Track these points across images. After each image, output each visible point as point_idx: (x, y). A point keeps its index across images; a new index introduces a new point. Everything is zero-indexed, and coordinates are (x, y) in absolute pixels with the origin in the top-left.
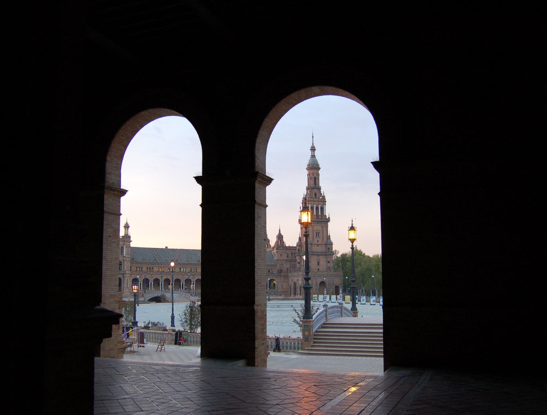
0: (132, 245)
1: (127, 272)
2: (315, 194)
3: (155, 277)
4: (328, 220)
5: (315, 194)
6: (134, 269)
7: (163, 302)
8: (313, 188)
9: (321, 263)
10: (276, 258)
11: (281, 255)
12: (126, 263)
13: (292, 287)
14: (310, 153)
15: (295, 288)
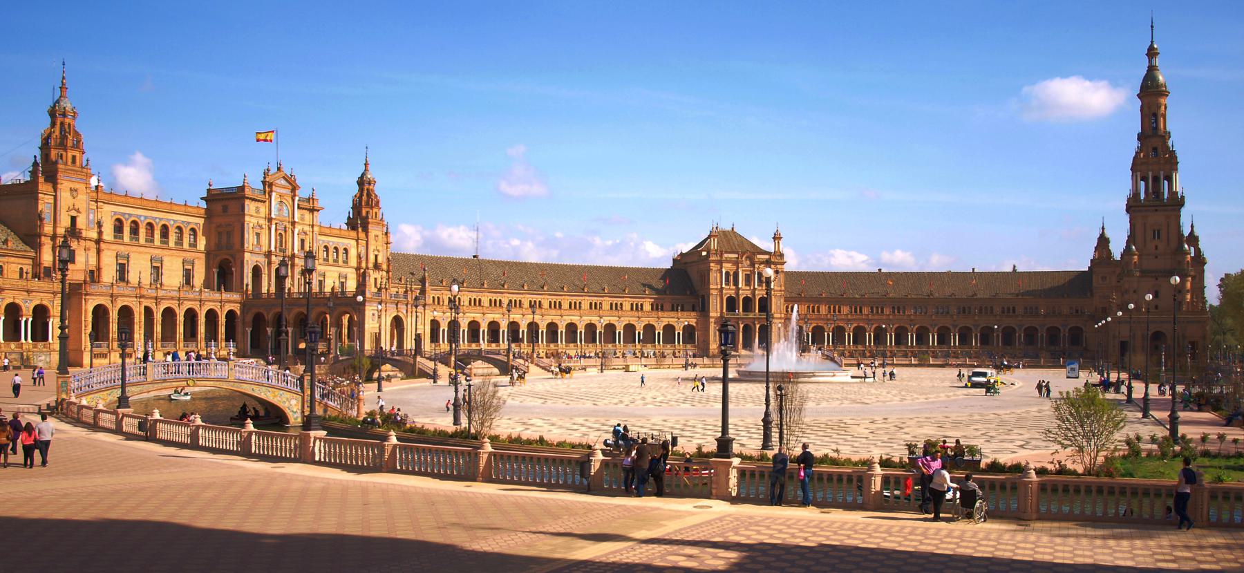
12: (774, 300)
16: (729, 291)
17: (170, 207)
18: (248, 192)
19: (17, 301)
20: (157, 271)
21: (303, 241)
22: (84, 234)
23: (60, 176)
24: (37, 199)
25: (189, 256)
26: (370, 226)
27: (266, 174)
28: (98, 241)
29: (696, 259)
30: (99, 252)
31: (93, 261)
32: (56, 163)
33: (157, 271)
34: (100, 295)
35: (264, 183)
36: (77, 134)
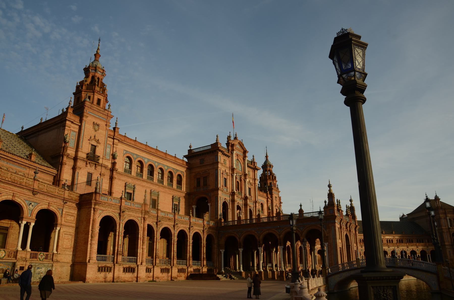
17: (165, 156)
18: (219, 146)
19: (18, 200)
21: (250, 189)
22: (100, 161)
23: (87, 110)
24: (64, 126)
26: (273, 191)
27: (229, 137)
32: (85, 101)
33: (154, 204)
34: (110, 205)
35: (228, 144)
36: (103, 85)
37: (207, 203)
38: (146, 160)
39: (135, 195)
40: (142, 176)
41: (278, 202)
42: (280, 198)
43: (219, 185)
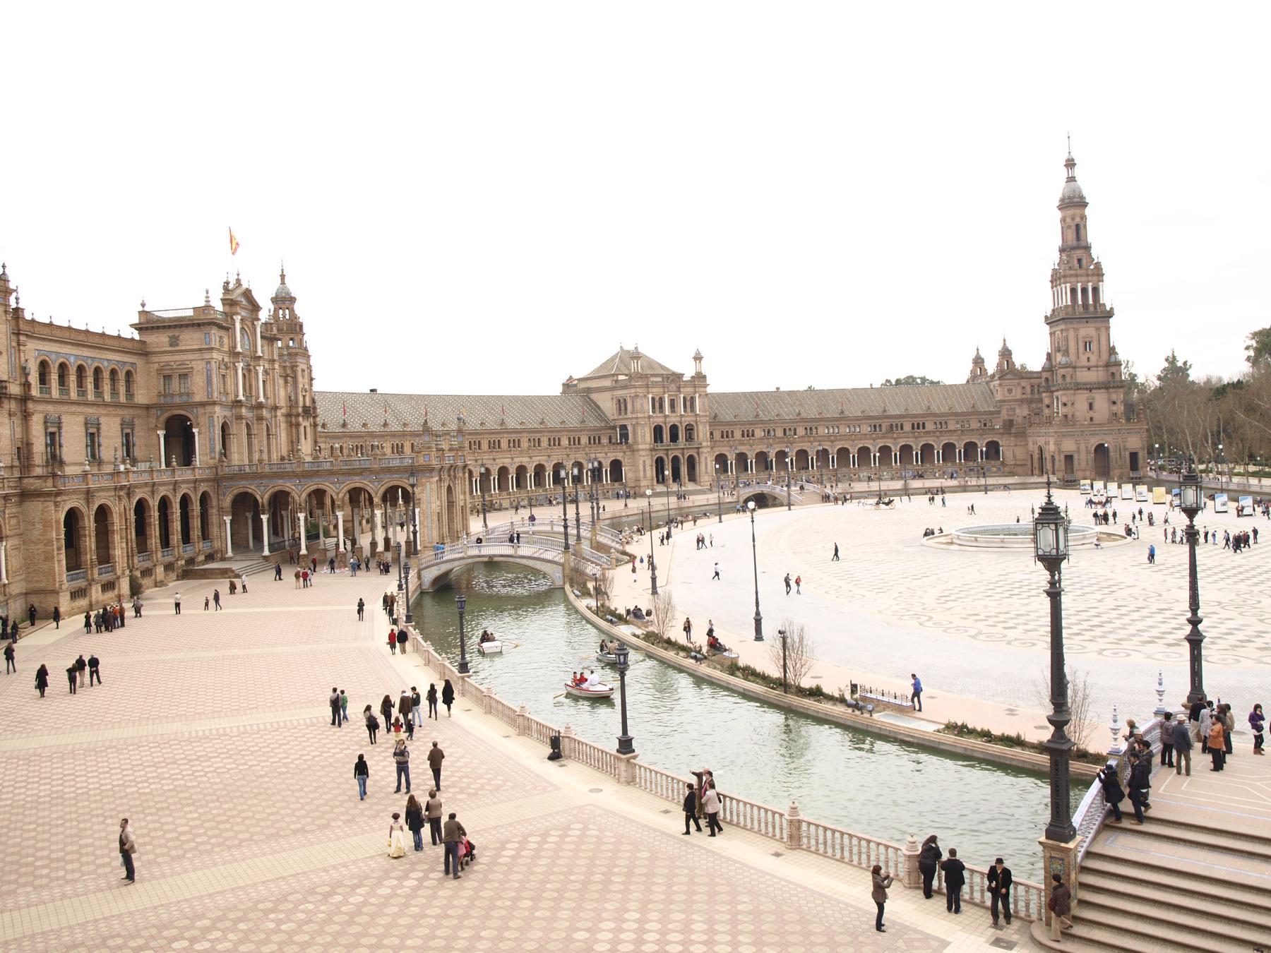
0: (709, 390)
1: (704, 444)
2: (1079, 261)
3: (759, 449)
4: (1110, 314)
5: (1079, 261)
6: (717, 435)
7: (774, 506)
8: (1073, 248)
9: (1096, 406)
10: (999, 397)
11: (1010, 391)
12: (701, 427)
13: (1036, 457)
14: (1064, 173)
15: (1041, 459)
16: (659, 420)
17: (101, 341)
20: (93, 440)
25: (127, 413)
28: (25, 399)
29: (607, 383)
30: (26, 416)
31: (18, 430)
37: (191, 426)
38: (72, 359)
39: (63, 434)
40: (68, 394)
41: (306, 380)
42: (310, 368)
43: (215, 394)
